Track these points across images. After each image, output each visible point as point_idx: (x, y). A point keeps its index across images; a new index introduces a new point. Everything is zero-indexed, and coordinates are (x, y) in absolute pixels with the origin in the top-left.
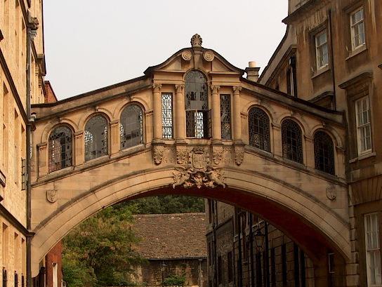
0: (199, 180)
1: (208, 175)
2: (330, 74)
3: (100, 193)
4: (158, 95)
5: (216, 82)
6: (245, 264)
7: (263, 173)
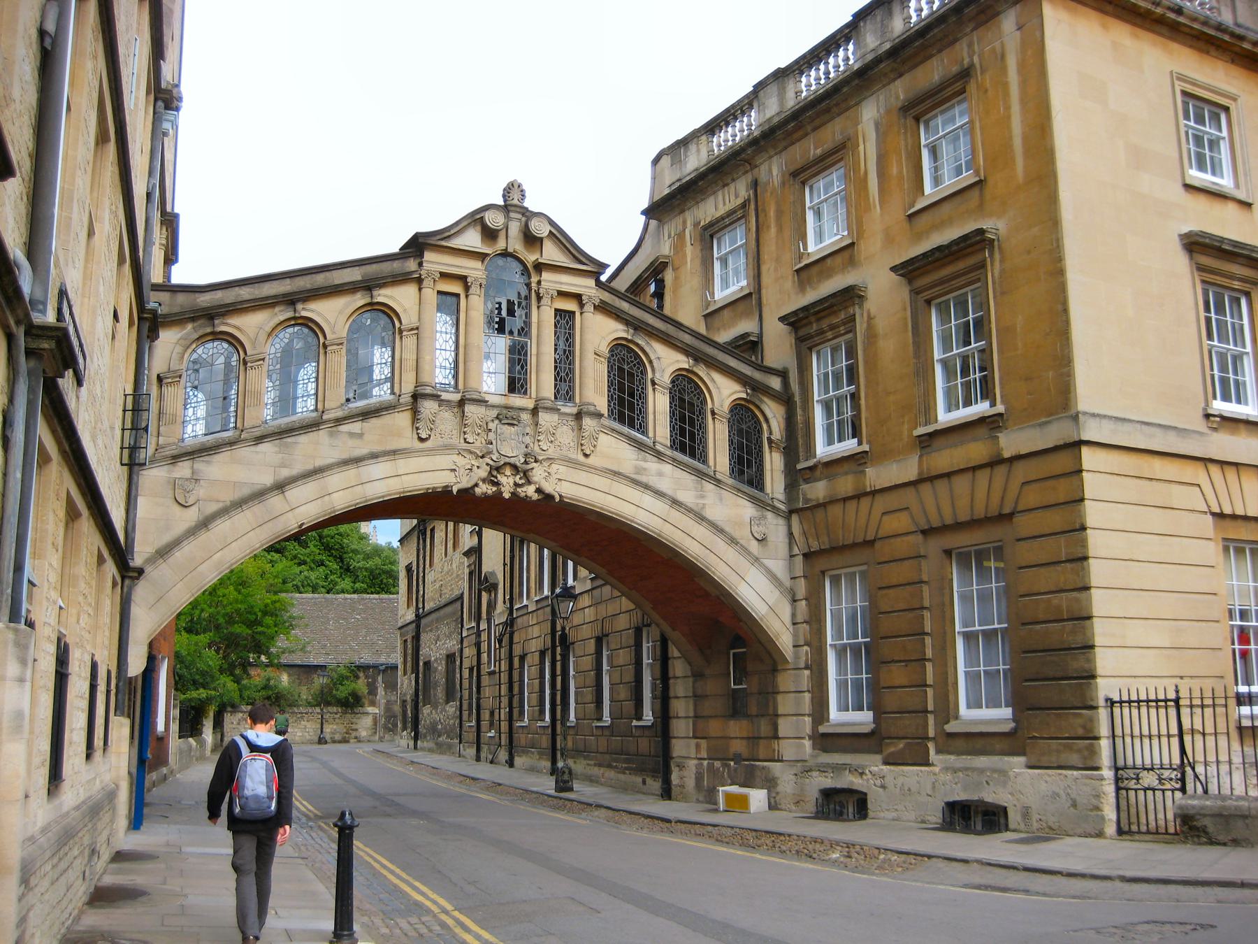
0: (507, 482)
2: (750, 301)
3: (296, 493)
6: (491, 673)
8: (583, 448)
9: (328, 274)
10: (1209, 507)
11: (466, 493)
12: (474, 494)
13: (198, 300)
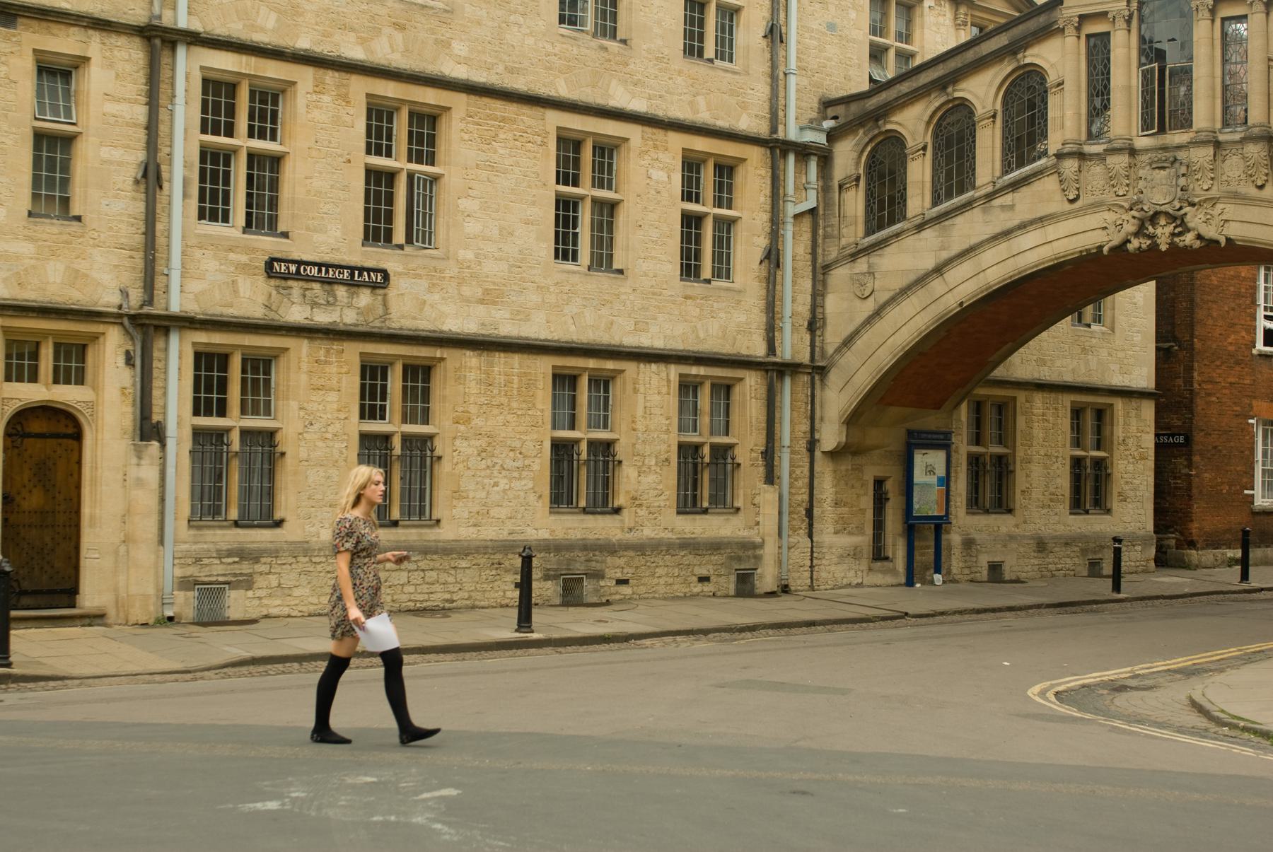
0: (1163, 232)
4: (1070, 40)
8: (1252, 179)
9: (976, 48)
12: (1127, 250)
13: (867, 105)
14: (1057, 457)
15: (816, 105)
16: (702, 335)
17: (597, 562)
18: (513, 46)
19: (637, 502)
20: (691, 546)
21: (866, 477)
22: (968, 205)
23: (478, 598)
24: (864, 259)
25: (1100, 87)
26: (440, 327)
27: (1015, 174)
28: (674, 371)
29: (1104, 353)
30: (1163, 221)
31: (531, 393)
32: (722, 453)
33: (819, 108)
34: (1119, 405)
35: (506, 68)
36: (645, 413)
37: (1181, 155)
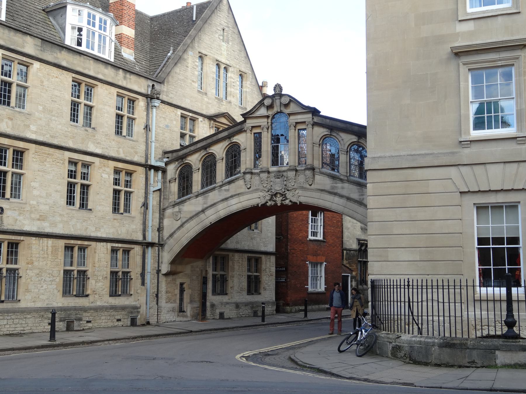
0: (279, 200)
1: (285, 195)
3: (209, 212)
5: (293, 119)
7: (330, 190)
9: (217, 136)
10: (459, 189)
11: (264, 205)
14: (243, 275)
15: (161, 153)
16: (120, 233)
17: (80, 314)
18: (53, 128)
19: (95, 293)
20: (114, 308)
21: (177, 283)
22: (214, 189)
23: (34, 329)
24: (177, 207)
25: (258, 151)
26: (22, 229)
27: (230, 179)
28: (109, 245)
29: (258, 239)
30: (279, 196)
31: (56, 253)
32: (126, 274)
33: (162, 154)
34: (263, 257)
35: (50, 136)
36: (99, 260)
37: (285, 174)
